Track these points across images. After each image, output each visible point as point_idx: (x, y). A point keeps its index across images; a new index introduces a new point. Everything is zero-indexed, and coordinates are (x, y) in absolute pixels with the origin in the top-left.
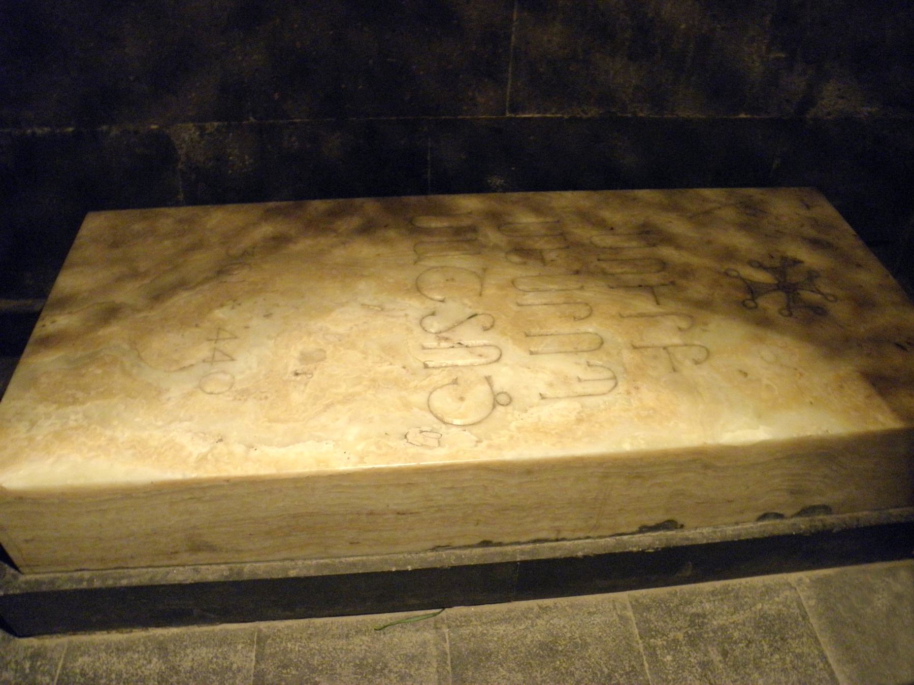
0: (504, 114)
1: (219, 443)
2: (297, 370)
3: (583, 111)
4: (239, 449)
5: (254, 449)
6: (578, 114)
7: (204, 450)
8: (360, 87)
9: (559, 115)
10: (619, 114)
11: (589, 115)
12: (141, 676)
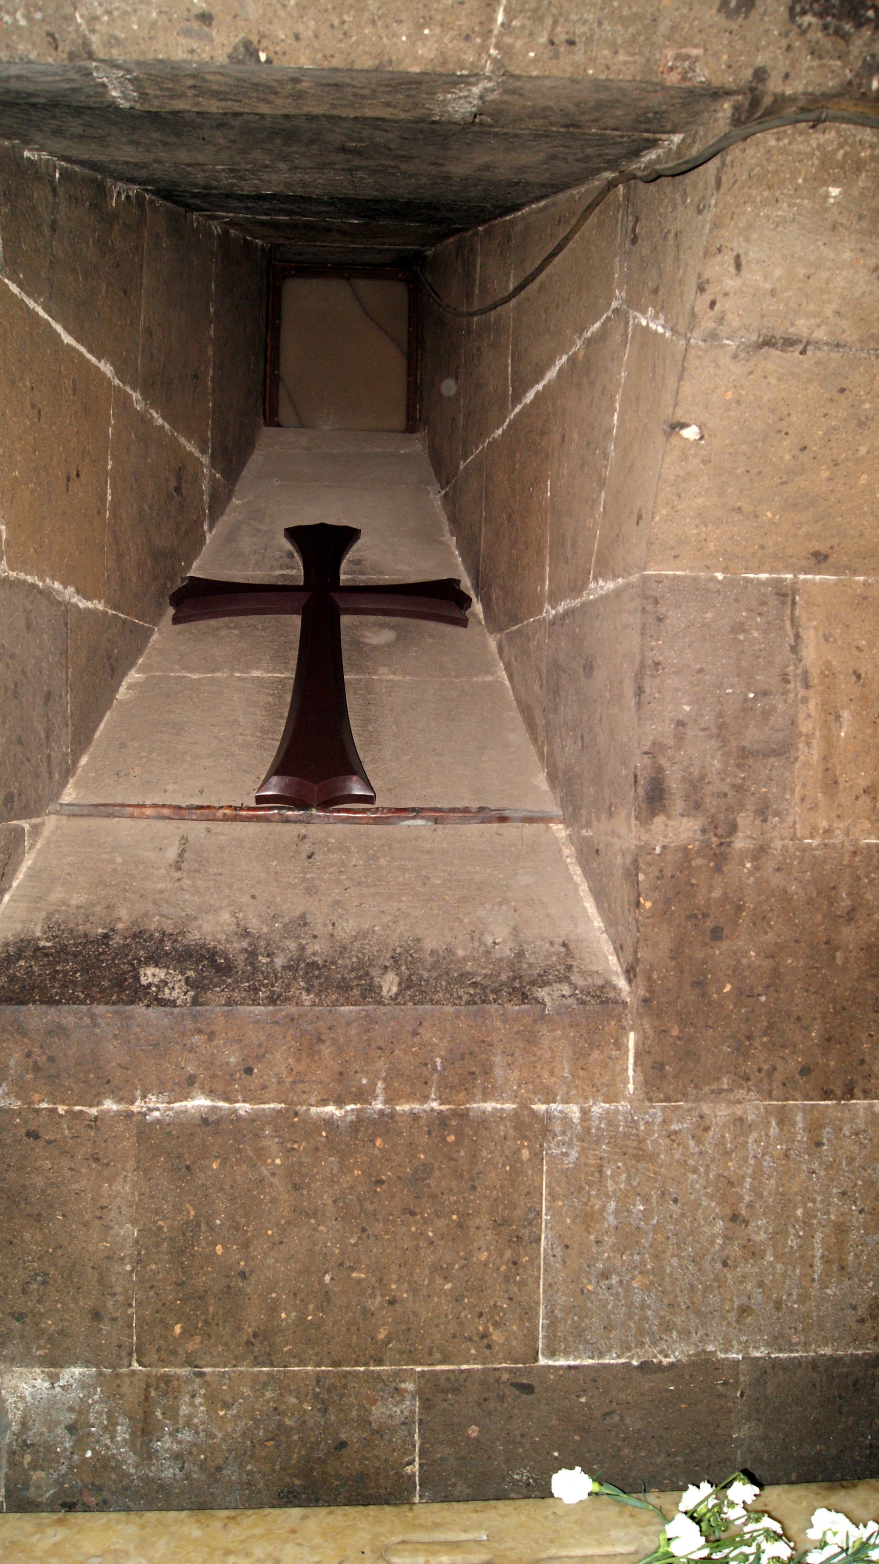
0: (536, 1360)
3: (661, 1352)
6: (656, 1357)
8: (310, 1318)
9: (622, 1361)
10: (721, 1356)
11: (672, 1359)
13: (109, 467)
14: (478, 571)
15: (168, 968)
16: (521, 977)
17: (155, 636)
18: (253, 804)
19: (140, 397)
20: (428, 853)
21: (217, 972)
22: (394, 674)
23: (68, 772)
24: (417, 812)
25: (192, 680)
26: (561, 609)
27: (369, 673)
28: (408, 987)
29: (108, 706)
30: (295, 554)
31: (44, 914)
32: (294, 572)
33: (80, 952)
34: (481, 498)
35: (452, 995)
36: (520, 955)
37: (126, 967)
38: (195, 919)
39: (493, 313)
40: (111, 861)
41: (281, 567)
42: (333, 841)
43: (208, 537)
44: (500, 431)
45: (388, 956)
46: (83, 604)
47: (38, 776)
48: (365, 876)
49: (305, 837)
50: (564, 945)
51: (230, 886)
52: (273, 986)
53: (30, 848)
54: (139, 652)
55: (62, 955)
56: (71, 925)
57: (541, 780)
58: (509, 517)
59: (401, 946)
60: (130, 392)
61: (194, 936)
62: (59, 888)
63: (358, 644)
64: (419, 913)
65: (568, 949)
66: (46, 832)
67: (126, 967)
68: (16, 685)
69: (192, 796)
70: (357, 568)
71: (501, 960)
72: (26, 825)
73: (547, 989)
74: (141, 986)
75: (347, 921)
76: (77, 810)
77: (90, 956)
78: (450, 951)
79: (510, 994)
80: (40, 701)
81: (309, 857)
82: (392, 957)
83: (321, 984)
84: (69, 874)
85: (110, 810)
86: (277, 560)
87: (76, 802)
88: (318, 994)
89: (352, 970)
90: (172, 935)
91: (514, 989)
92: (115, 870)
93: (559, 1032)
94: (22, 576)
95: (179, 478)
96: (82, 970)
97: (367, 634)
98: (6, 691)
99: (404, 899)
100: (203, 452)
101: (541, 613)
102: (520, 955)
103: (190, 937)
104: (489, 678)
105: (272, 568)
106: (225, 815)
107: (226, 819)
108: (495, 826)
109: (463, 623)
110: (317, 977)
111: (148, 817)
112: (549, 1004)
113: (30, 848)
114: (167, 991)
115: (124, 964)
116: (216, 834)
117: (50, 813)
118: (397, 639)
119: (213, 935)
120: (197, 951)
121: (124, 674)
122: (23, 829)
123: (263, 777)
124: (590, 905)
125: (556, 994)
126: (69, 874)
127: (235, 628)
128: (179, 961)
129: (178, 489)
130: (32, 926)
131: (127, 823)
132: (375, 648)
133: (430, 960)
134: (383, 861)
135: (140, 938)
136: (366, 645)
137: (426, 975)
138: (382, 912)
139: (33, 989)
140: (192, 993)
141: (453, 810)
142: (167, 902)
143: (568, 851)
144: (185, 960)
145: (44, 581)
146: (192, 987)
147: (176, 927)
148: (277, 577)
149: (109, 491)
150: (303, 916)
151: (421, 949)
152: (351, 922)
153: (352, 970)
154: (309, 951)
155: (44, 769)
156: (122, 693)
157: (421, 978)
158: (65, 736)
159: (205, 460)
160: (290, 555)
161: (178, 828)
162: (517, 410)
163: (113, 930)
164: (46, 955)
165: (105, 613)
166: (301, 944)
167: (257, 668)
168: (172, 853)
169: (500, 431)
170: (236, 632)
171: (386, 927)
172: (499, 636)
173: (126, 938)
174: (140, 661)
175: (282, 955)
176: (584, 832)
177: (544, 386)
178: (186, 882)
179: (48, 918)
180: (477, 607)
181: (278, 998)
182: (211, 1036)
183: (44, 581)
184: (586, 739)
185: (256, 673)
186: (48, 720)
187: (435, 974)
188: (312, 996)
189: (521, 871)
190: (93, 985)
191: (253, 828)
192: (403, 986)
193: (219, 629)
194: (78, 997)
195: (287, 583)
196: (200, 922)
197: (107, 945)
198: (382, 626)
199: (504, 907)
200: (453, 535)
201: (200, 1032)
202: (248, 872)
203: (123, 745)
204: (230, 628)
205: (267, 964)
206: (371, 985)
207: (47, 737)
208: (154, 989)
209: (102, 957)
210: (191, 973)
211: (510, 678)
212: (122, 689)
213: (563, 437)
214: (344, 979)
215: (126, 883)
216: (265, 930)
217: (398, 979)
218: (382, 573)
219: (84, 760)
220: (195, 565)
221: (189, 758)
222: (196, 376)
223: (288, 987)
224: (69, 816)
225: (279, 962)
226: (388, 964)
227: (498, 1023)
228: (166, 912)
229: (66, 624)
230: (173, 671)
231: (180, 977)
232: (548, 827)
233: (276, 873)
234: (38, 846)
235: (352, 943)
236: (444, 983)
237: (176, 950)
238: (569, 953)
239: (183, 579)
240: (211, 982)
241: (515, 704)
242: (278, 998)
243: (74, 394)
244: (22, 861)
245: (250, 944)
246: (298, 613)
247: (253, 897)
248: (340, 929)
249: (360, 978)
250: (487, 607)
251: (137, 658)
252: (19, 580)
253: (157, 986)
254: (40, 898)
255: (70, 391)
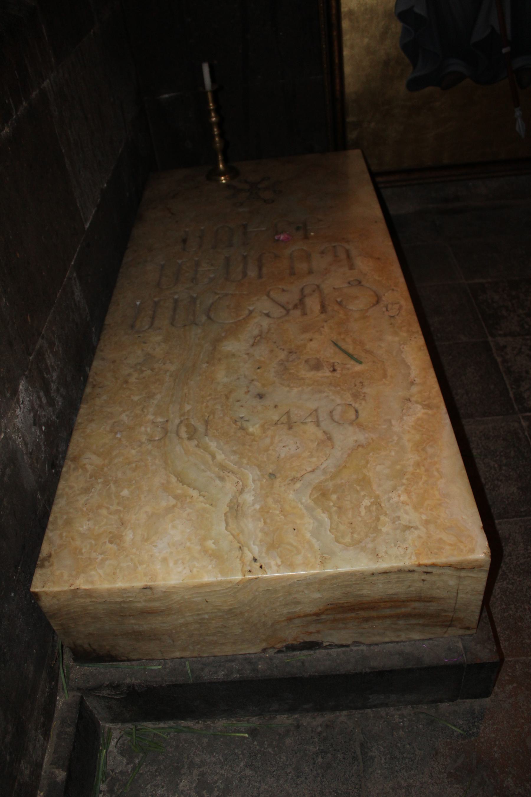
1: (411, 400)
2: (330, 371)
4: (414, 389)
5: (414, 381)
7: (419, 407)
12: (502, 594)
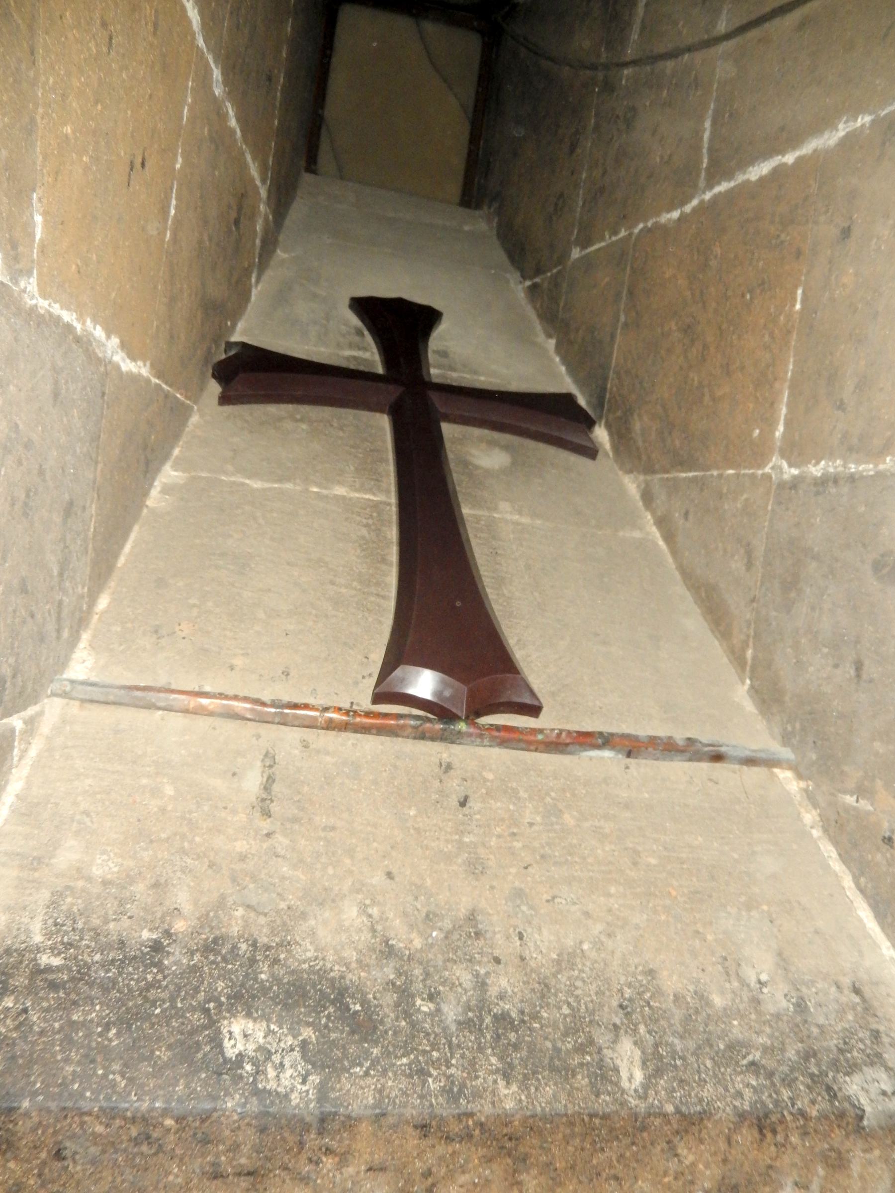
13: (178, 166)
14: (604, 389)
15: (269, 1020)
16: (815, 1055)
17: (195, 419)
18: (365, 702)
19: (220, 78)
20: (627, 806)
21: (353, 1032)
22: (520, 513)
23: (82, 622)
24: (605, 741)
25: (253, 491)
26: (816, 470)
27: (489, 509)
28: (658, 1072)
29: (136, 518)
30: (366, 333)
31: (45, 895)
32: (367, 355)
33: (114, 982)
34: (618, 295)
35: (726, 1089)
36: (801, 1006)
37: (197, 1018)
38: (304, 916)
39: (670, 65)
40: (156, 792)
41: (351, 346)
42: (490, 776)
43: (254, 292)
44: (675, 214)
45: (615, 1003)
46: (128, 366)
47: (42, 640)
48: (548, 844)
49: (449, 767)
50: (857, 991)
51: (351, 852)
52: (448, 1065)
53: (20, 760)
54: (177, 436)
55: (83, 987)
56: (96, 922)
57: (741, 693)
58: (687, 329)
59: (630, 985)
60: (213, 66)
61: (305, 951)
62: (72, 842)
63: (466, 464)
64: (639, 919)
65: (864, 1000)
66: (45, 727)
67: (197, 1018)
68: (28, 496)
69: (273, 679)
70: (444, 361)
71: (778, 1017)
72: (16, 722)
73: (857, 1078)
74: (226, 1061)
75: (540, 929)
76: (96, 693)
77: (130, 990)
78: (701, 996)
79: (808, 1087)
80: (57, 518)
81: (463, 803)
82: (621, 1006)
83: (524, 1062)
84: (86, 813)
85: (152, 696)
86: (344, 336)
87: (94, 679)
88: (524, 1086)
89: (566, 1034)
90: (268, 948)
91: (812, 1076)
92: (163, 810)
93: (877, 1152)
94: (56, 309)
95: (240, 208)
96: (120, 1021)
97: (474, 451)
98: (13, 505)
99: (613, 890)
100: (263, 181)
101: (760, 466)
102: (801, 1006)
103: (297, 950)
104: (637, 534)
105: (339, 346)
106: (331, 720)
107: (330, 726)
108: (705, 766)
109: (590, 452)
110: (516, 1047)
111: (211, 714)
112: (868, 1109)
113: (20, 760)
114: (271, 1073)
115: (193, 1009)
116: (318, 752)
117: (54, 694)
118: (514, 463)
119: (336, 952)
120: (314, 986)
121: (158, 470)
122: (13, 731)
123: (378, 656)
124: (865, 913)
125: (874, 1089)
126: (86, 813)
127: (302, 420)
128: (286, 1007)
129: (237, 222)
130: (26, 920)
131: (177, 721)
132: (488, 472)
133: (678, 1015)
134: (569, 819)
135: (217, 953)
136: (477, 467)
137: (678, 1045)
138: (587, 914)
139: (30, 1063)
140: (315, 1079)
141: (653, 741)
142: (254, 878)
143: (809, 817)
144: (296, 1004)
145: (84, 324)
146: (314, 1065)
147: (273, 933)
148: (348, 359)
149: (174, 202)
150: (472, 917)
151: (658, 992)
152: (545, 932)
153: (566, 1034)
154: (493, 991)
155: (51, 627)
156: (155, 498)
157: (674, 1054)
158: (82, 566)
159: (263, 193)
160: (359, 333)
161: (258, 736)
162: (723, 187)
163: (168, 934)
164: (54, 986)
165: (148, 381)
166: (477, 975)
167: (339, 483)
168: (252, 782)
169: (675, 214)
170: (304, 426)
171: (598, 946)
172: (642, 478)
173: (192, 953)
174: (176, 452)
175: (452, 997)
176: (850, 800)
177: (800, 160)
178: (281, 841)
179: (53, 904)
180: (601, 434)
181: (460, 1091)
182: (344, 1158)
183: (84, 324)
184: (871, 670)
185: (340, 491)
186: (66, 547)
187: (692, 1045)
188: (514, 1088)
189: (758, 848)
190: (143, 1058)
191: (371, 744)
192: (651, 1067)
193: (281, 419)
194: (114, 1085)
195: (362, 368)
196: (312, 922)
197: (159, 965)
198: (492, 443)
199: (754, 913)
200: (549, 336)
201: (329, 1151)
202: (375, 826)
203: (161, 583)
204: (297, 421)
205: (430, 1014)
206: (601, 1064)
207: (61, 574)
208: (248, 1067)
209: (152, 994)
210: (308, 1033)
211: (669, 537)
212: (155, 492)
213: (846, 233)
214: (557, 1050)
215: (183, 837)
216: (418, 943)
217: (638, 1053)
218: (475, 372)
219: (103, 602)
220: (240, 326)
221: (261, 615)
222: (269, 79)
223: (472, 1067)
224: (83, 701)
225: (451, 1012)
226: (618, 1022)
227: (795, 1139)
228: (254, 901)
229: (103, 394)
230: (225, 473)
231: (290, 1040)
232: (773, 774)
233: (417, 830)
234: (33, 752)
235: (555, 976)
236: (709, 1063)
237: (277, 980)
238: (868, 1008)
239: (229, 345)
240: (345, 1055)
241: (677, 576)
242: (460, 1091)
243: (155, 34)
244: (7, 782)
245: (399, 974)
246: (382, 411)
247: (390, 875)
248: (531, 945)
249: (580, 1049)
250: (621, 436)
251: (172, 448)
252: (51, 315)
253: (255, 1062)
254: (39, 859)
255: (150, 27)
